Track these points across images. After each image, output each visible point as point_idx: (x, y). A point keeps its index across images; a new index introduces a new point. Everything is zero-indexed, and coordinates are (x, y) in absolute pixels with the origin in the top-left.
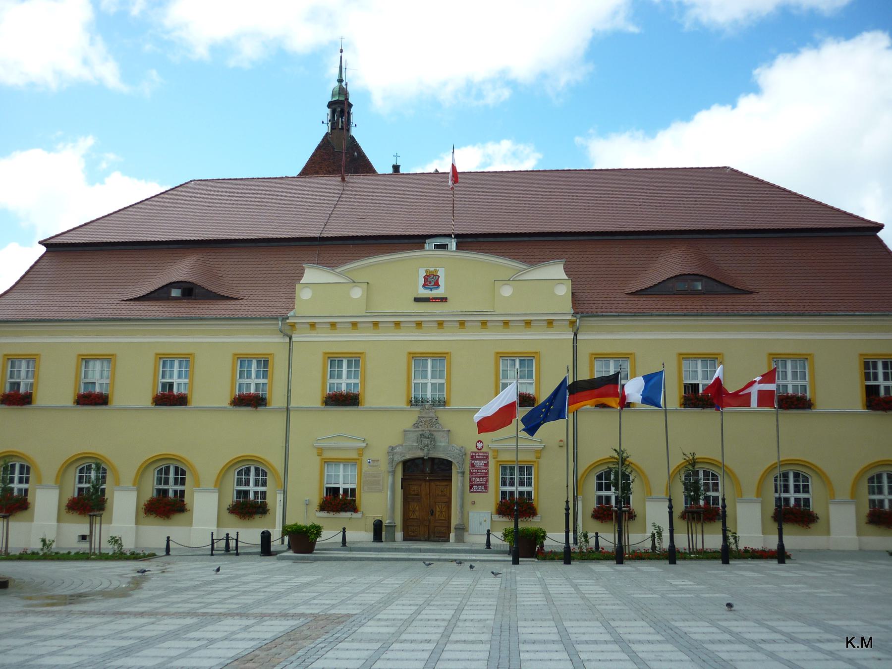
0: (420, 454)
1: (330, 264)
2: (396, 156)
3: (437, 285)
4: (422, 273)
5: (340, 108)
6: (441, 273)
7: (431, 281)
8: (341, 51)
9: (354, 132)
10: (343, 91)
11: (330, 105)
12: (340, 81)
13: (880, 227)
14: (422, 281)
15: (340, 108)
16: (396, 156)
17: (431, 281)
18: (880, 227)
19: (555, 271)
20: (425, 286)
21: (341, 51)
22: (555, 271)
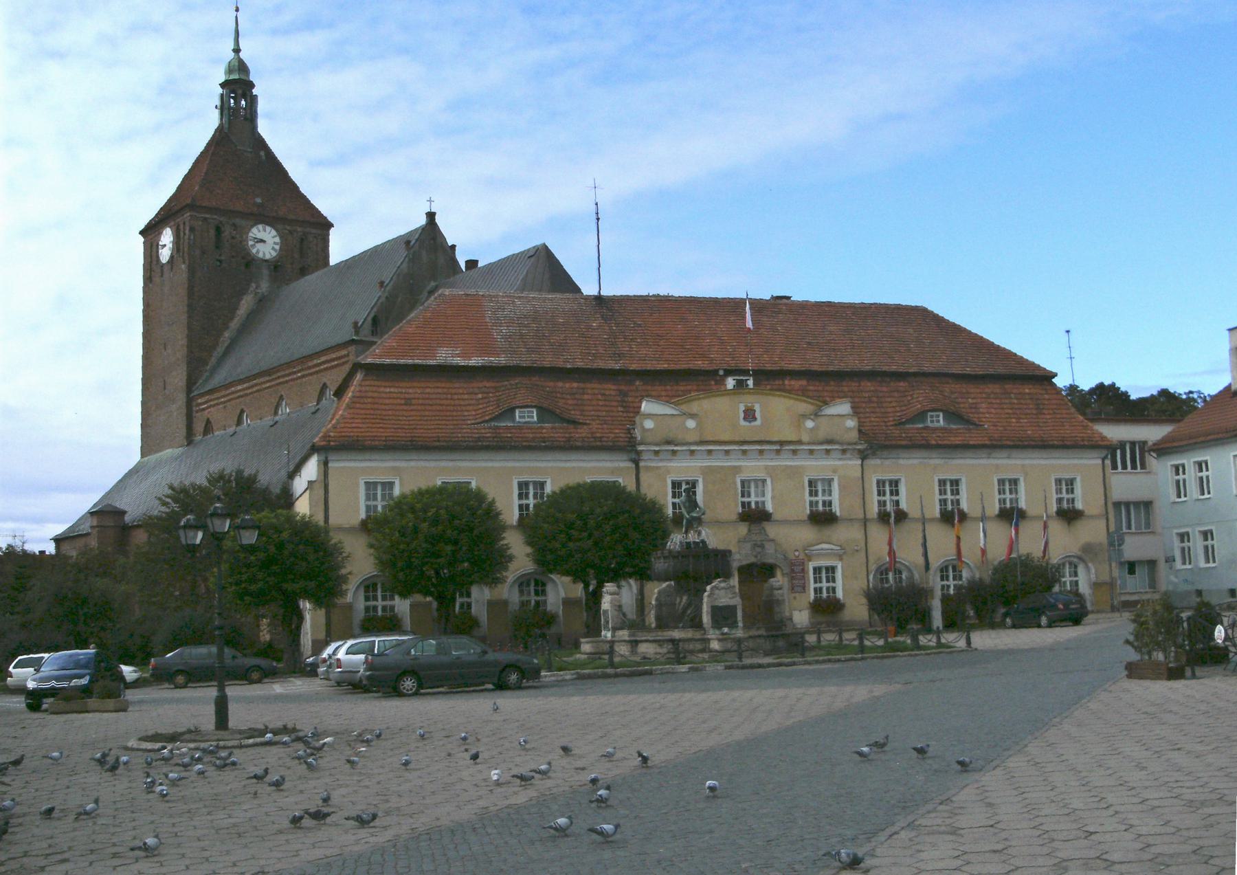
0: (753, 560)
1: (668, 400)
2: (430, 201)
3: (755, 419)
4: (742, 407)
5: (239, 88)
6: (757, 407)
7: (749, 415)
8: (237, 10)
9: (264, 128)
10: (242, 67)
11: (223, 85)
12: (237, 51)
13: (1055, 375)
14: (742, 415)
15: (239, 88)
16: (430, 201)
17: (749, 415)
18: (1055, 375)
19: (843, 408)
20: (745, 419)
21: (237, 10)
22: (843, 408)
